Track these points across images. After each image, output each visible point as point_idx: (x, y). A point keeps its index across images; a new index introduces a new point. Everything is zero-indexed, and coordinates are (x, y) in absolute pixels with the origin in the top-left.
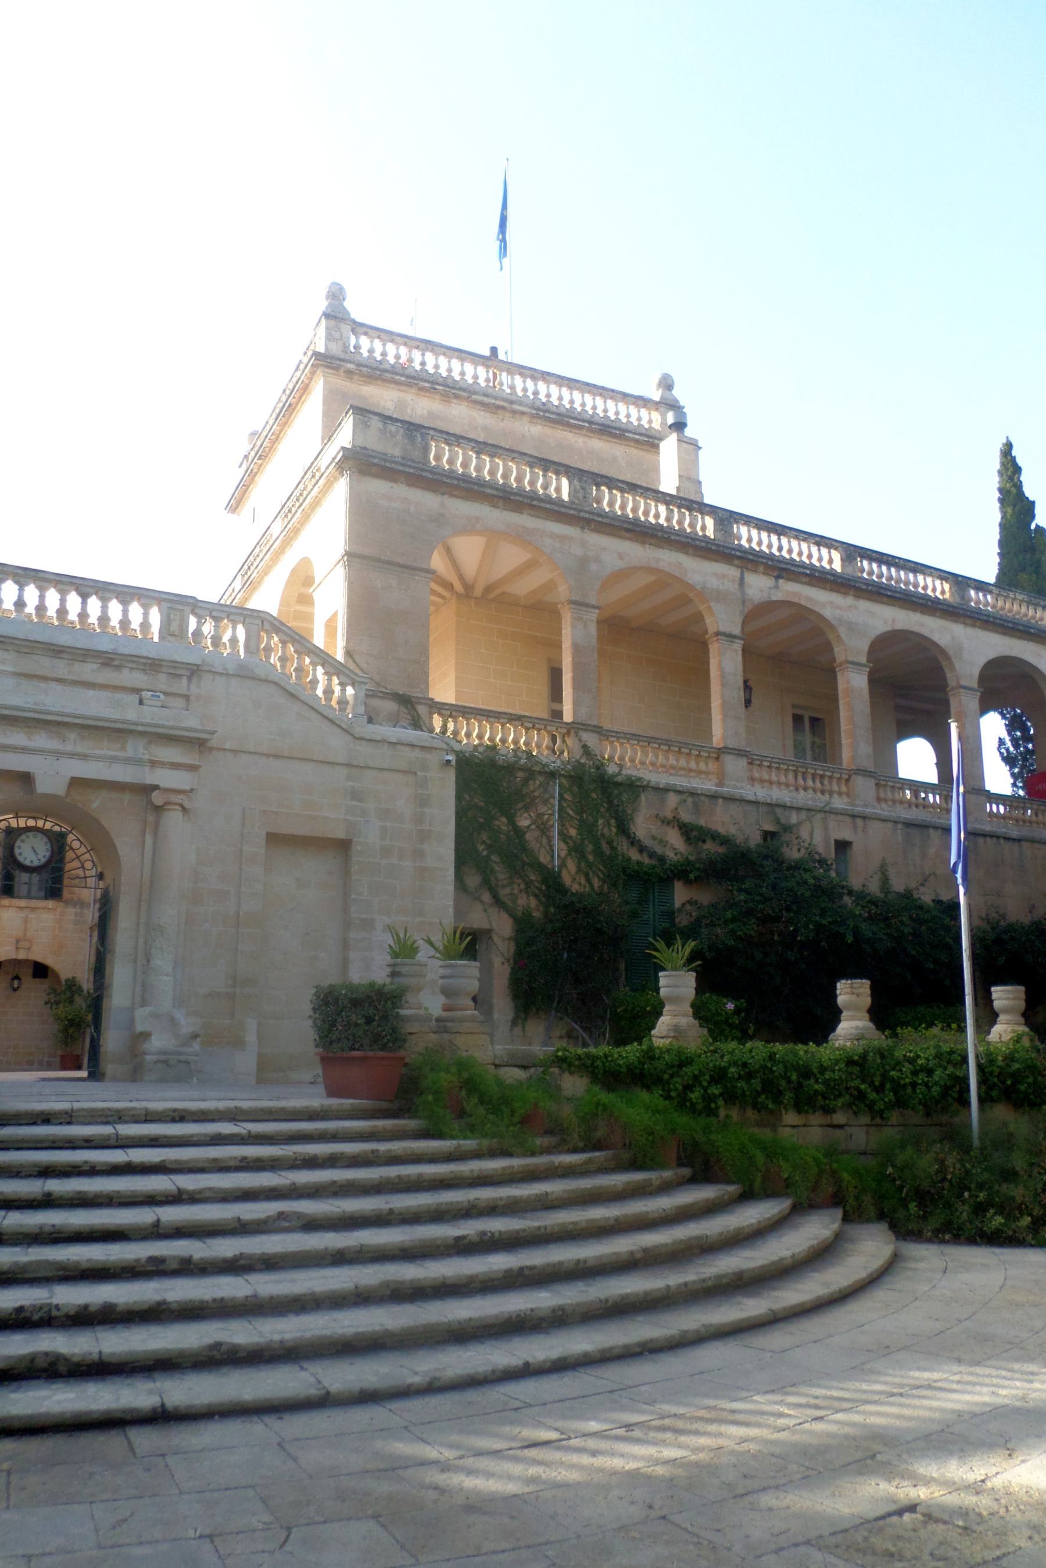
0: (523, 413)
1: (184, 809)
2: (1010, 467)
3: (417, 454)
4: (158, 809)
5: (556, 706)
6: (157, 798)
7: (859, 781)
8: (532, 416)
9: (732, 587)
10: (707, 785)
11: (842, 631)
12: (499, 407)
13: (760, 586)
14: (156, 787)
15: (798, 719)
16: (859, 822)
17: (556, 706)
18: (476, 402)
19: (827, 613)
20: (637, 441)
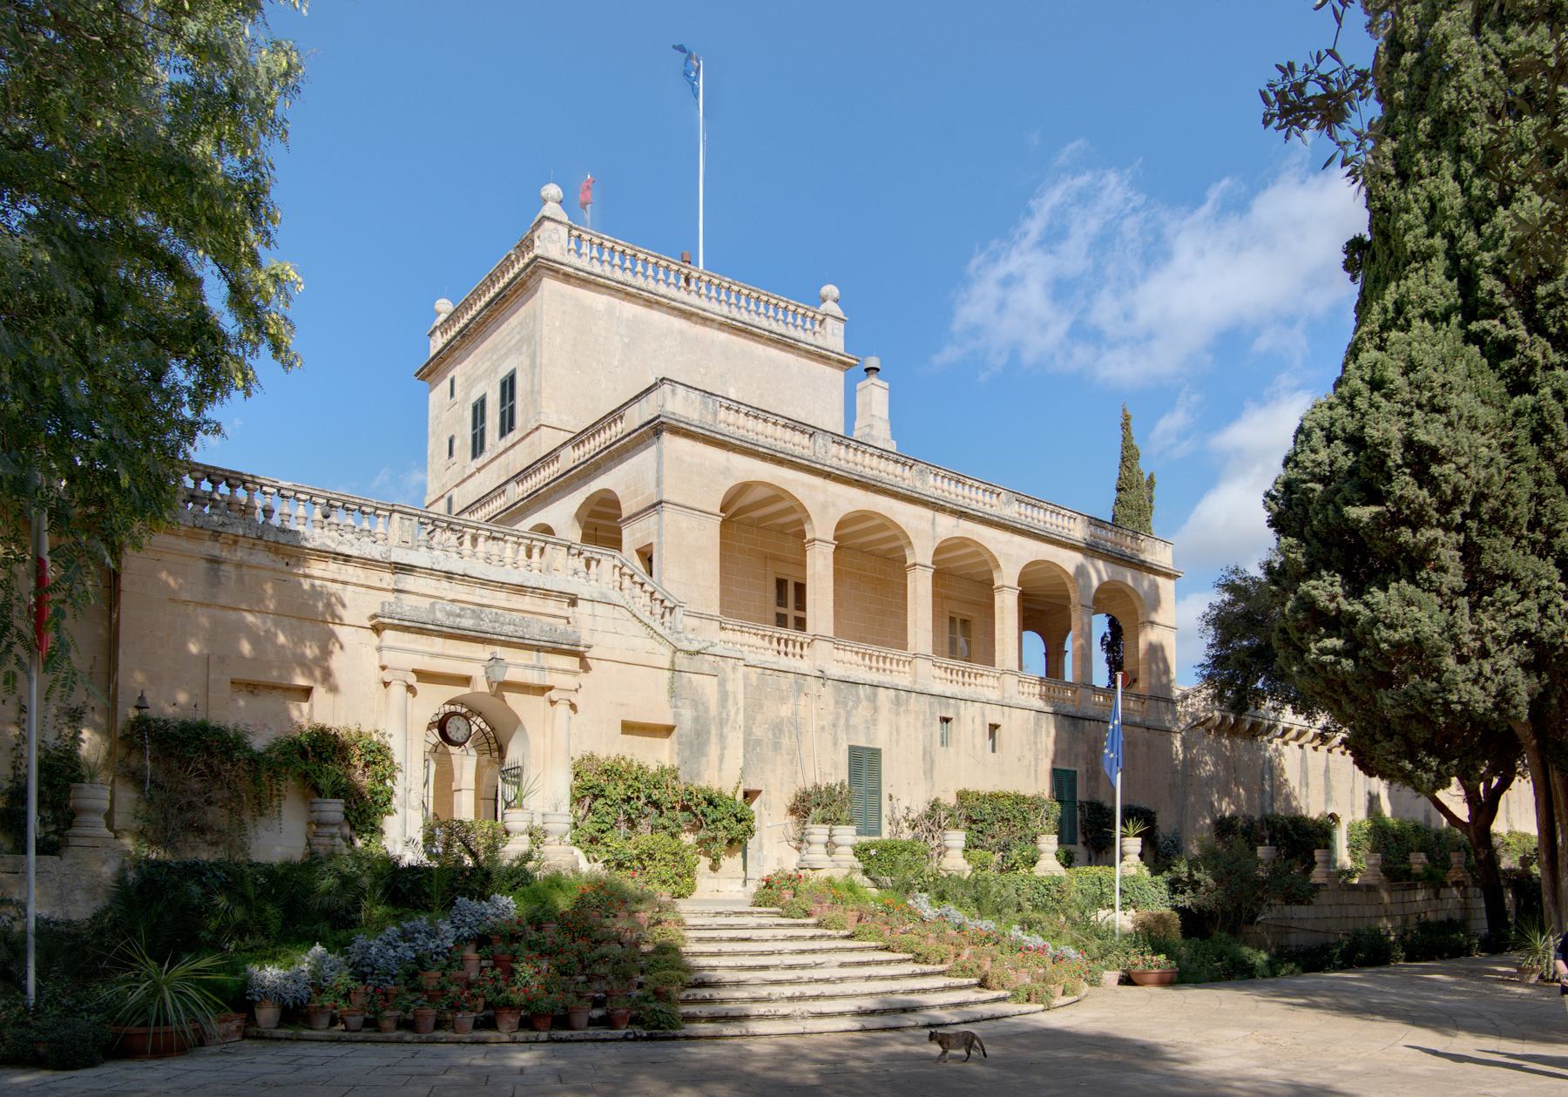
0: (713, 320)
1: (573, 707)
2: (1127, 419)
3: (709, 419)
4: (553, 703)
5: (782, 610)
7: (1007, 677)
8: (721, 324)
9: (926, 526)
10: (904, 681)
11: (1001, 561)
12: (692, 314)
13: (949, 527)
14: (551, 688)
15: (952, 620)
17: (782, 610)
18: (674, 308)
19: (991, 547)
20: (808, 352)
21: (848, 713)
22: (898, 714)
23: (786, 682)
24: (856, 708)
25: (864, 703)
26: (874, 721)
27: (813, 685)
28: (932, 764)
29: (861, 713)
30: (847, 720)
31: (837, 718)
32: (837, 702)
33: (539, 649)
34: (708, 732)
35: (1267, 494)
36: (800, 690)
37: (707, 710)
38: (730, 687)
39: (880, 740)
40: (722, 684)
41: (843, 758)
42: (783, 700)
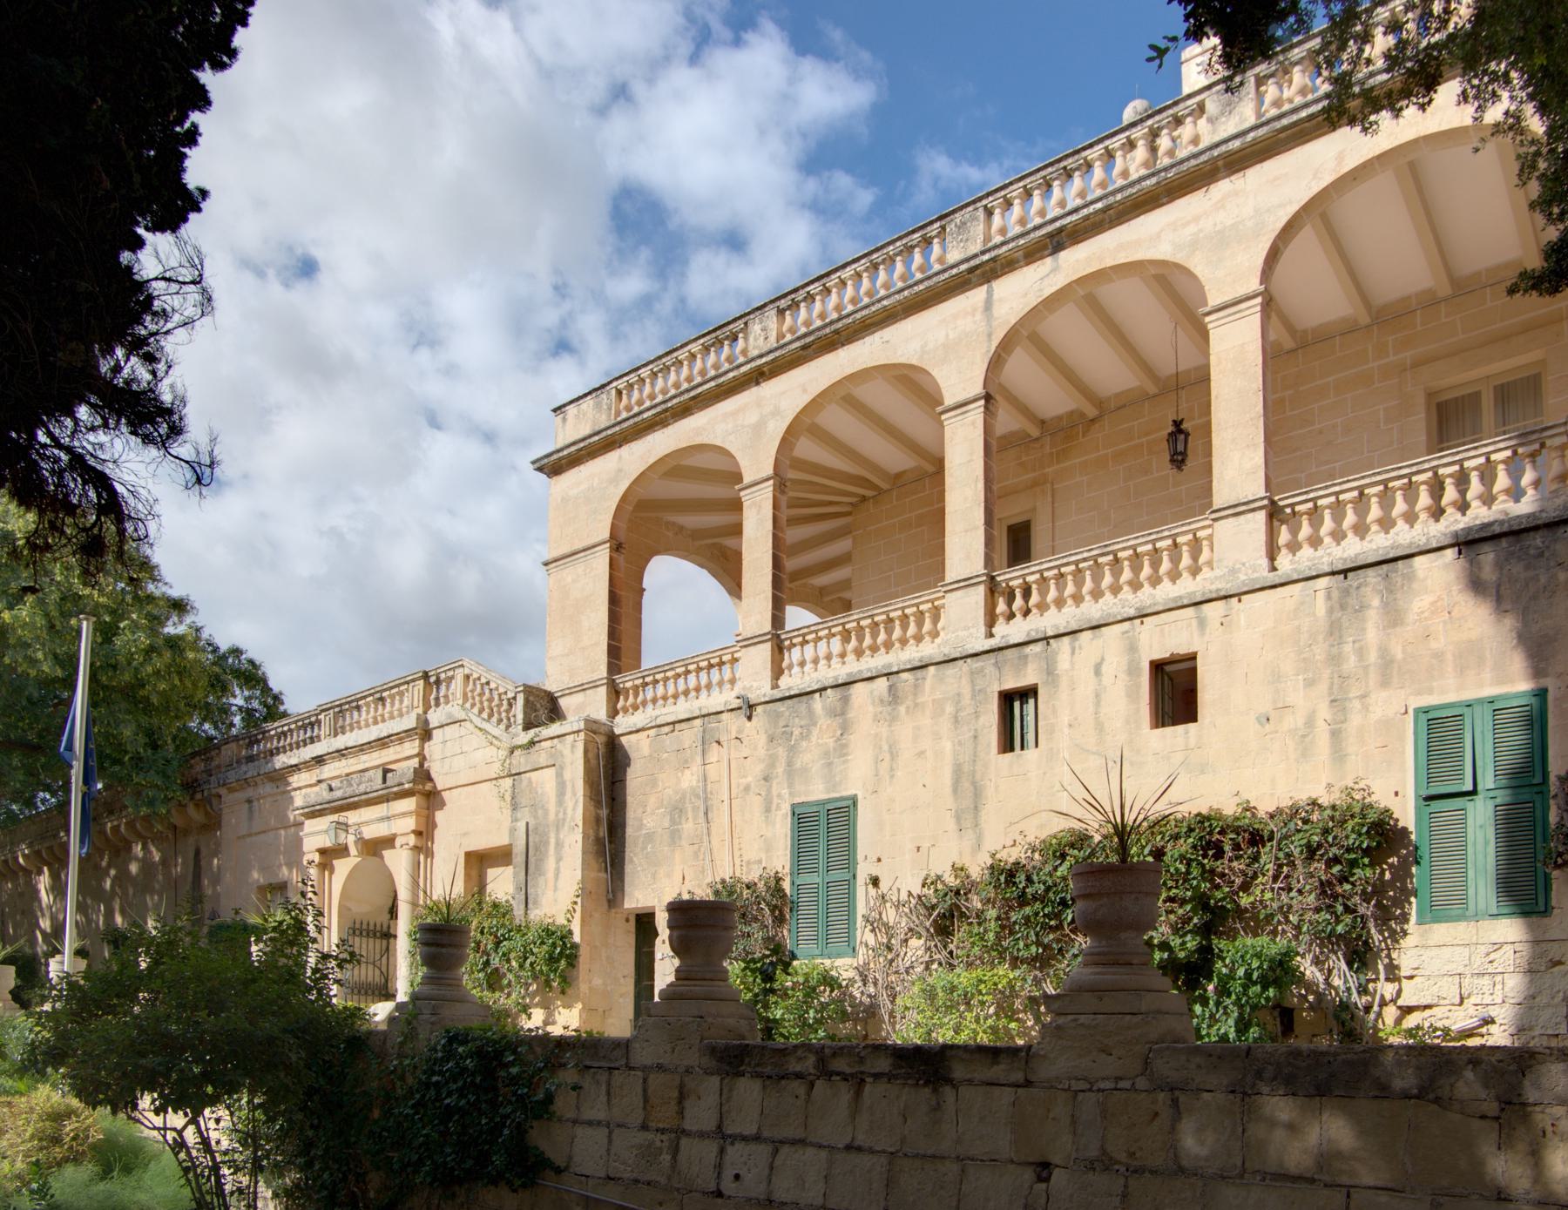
6: (398, 842)
16: (1213, 611)
21: (793, 750)
22: (893, 719)
23: (689, 736)
24: (805, 736)
25: (823, 721)
26: (842, 749)
27: (733, 723)
28: (977, 793)
29: (823, 735)
30: (790, 764)
31: (772, 762)
32: (771, 739)
33: (386, 799)
34: (547, 843)
35: (245, 25)
36: (709, 741)
37: (546, 812)
38: (567, 775)
39: (855, 780)
40: (559, 775)
41: (781, 829)
42: (685, 765)
